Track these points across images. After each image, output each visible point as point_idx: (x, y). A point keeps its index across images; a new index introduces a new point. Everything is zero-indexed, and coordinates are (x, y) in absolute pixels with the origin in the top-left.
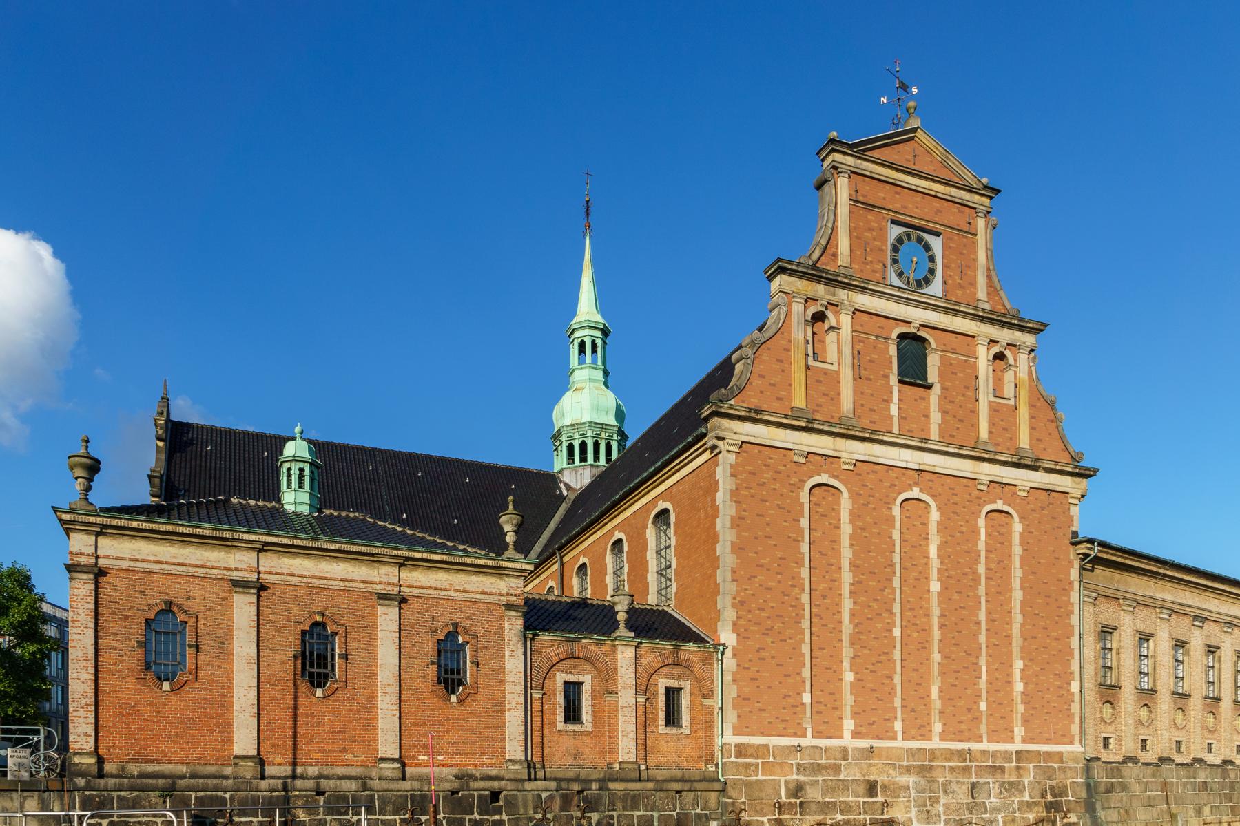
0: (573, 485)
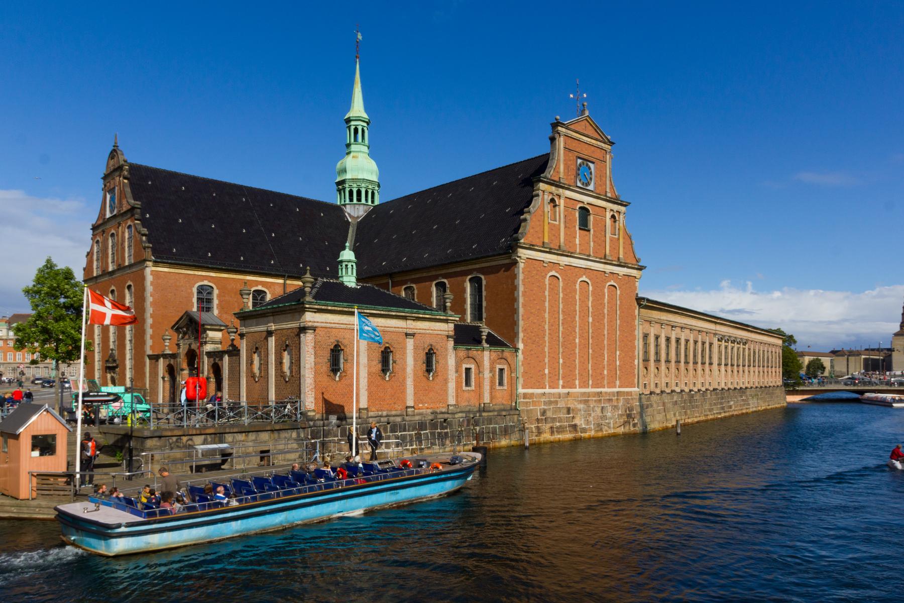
0: (352, 214)
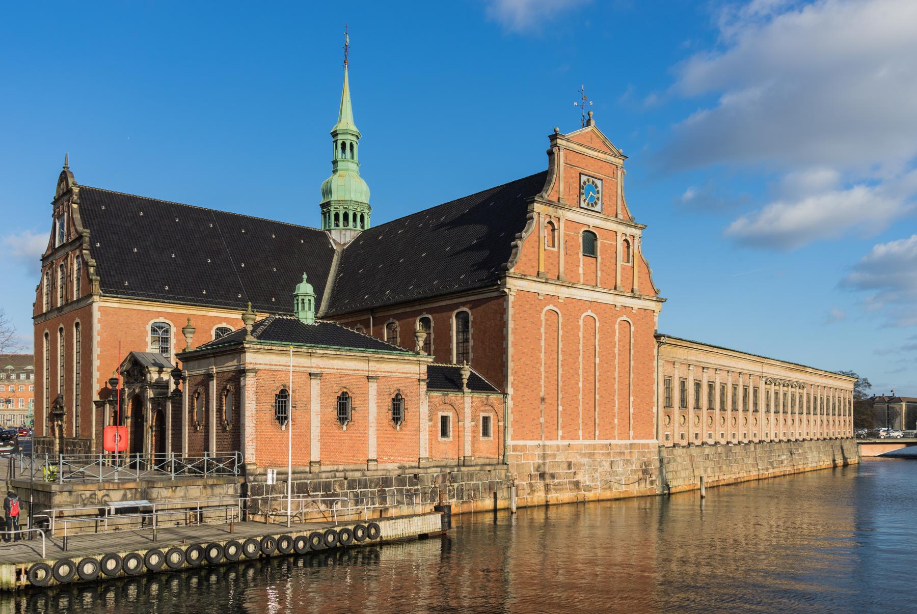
0: (338, 240)
